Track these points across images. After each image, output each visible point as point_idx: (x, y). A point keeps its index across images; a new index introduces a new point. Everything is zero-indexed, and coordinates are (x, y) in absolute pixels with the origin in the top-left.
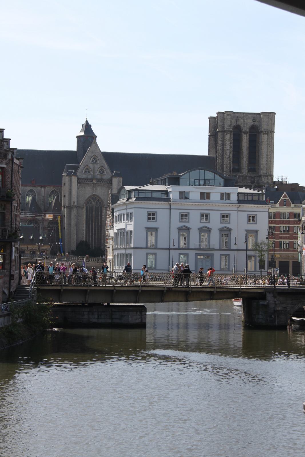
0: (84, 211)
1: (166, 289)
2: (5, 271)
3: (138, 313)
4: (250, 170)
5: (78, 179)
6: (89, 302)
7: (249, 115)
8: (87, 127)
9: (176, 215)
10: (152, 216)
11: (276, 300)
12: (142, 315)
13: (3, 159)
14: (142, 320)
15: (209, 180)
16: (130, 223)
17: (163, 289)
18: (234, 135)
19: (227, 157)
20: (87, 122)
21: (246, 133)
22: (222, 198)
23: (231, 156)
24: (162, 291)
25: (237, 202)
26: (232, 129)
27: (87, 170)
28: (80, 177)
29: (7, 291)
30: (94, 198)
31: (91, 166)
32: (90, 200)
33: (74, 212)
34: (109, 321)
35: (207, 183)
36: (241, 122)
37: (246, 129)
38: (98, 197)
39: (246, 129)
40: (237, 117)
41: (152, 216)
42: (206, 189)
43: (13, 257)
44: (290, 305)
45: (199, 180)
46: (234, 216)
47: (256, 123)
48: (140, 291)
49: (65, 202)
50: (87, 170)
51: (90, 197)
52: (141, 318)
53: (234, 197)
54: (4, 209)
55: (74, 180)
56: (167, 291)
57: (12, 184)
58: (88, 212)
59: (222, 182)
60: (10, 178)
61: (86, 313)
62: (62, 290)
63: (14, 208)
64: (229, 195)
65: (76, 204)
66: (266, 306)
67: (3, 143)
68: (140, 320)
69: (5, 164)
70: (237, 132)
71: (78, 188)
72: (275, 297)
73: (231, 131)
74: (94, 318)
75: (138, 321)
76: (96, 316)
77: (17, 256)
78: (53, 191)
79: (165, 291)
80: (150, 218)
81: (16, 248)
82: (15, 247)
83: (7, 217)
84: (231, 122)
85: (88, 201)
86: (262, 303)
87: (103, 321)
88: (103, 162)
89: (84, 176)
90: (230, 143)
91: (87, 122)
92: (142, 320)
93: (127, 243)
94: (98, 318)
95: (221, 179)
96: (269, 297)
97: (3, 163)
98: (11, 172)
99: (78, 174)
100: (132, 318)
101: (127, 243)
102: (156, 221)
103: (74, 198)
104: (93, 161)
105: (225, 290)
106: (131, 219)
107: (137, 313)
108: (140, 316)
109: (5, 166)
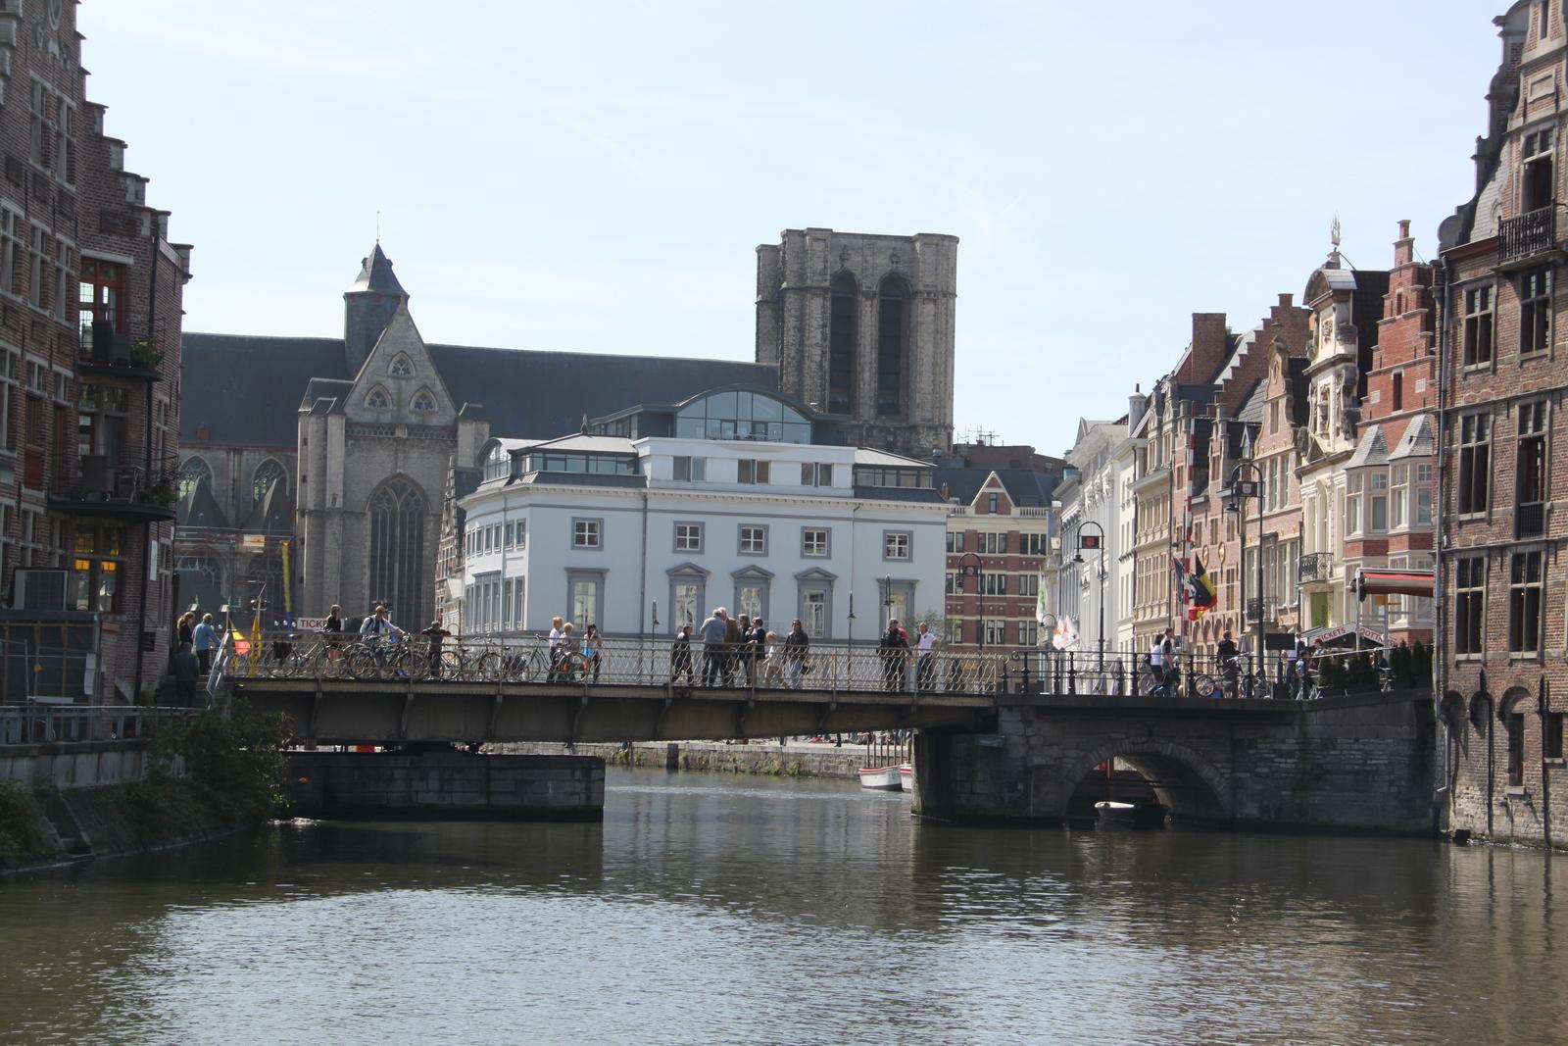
0: (367, 525)
1: (671, 693)
2: (125, 618)
3: (578, 774)
4: (882, 410)
5: (350, 426)
6: (412, 736)
7: (881, 243)
8: (380, 268)
9: (662, 530)
10: (586, 533)
11: (1029, 732)
12: (589, 782)
13: (121, 235)
14: (589, 798)
15: (766, 424)
16: (516, 554)
17: (661, 695)
18: (834, 301)
19: (814, 366)
20: (378, 250)
21: (870, 296)
22: (805, 479)
23: (826, 364)
24: (660, 702)
25: (851, 493)
26: (827, 284)
27: (379, 398)
28: (355, 419)
30: (399, 484)
31: (390, 384)
32: (385, 492)
33: (333, 528)
34: (481, 800)
35: (758, 431)
36: (854, 264)
37: (869, 283)
38: (412, 481)
39: (869, 283)
40: (845, 247)
41: (586, 533)
42: (756, 451)
43: (153, 576)
44: (1072, 753)
45: (735, 422)
46: (841, 534)
47: (902, 268)
48: (585, 701)
49: (306, 496)
50: (379, 398)
51: (385, 482)
52: (588, 789)
53: (842, 478)
54: (123, 406)
55: (336, 425)
56: (674, 700)
57: (151, 320)
58: (380, 529)
59: (806, 430)
60: (147, 302)
61: (398, 774)
62: (319, 695)
63: (160, 408)
64: (827, 469)
65: (339, 503)
66: (999, 753)
67: (121, 180)
68: (583, 796)
69: (128, 252)
70: (843, 293)
71: (348, 454)
72: (1027, 723)
73: (825, 290)
74: (428, 791)
75: (577, 801)
76: (434, 785)
77: (166, 576)
78: (265, 465)
79: (668, 702)
80: (580, 540)
81: (163, 545)
82: (158, 541)
83: (133, 436)
84: (825, 261)
85: (380, 495)
86: (986, 741)
87: (456, 799)
89: (368, 417)
90: (824, 326)
91: (378, 250)
92: (589, 798)
93: (506, 619)
94: (441, 791)
95: (804, 421)
96: (1009, 722)
97: (122, 251)
98: (148, 282)
99: (348, 409)
100: (555, 792)
101: (506, 619)
102: (601, 548)
104: (396, 370)
105: (864, 700)
106: (520, 540)
107: (573, 774)
108: (584, 785)
109: (130, 261)
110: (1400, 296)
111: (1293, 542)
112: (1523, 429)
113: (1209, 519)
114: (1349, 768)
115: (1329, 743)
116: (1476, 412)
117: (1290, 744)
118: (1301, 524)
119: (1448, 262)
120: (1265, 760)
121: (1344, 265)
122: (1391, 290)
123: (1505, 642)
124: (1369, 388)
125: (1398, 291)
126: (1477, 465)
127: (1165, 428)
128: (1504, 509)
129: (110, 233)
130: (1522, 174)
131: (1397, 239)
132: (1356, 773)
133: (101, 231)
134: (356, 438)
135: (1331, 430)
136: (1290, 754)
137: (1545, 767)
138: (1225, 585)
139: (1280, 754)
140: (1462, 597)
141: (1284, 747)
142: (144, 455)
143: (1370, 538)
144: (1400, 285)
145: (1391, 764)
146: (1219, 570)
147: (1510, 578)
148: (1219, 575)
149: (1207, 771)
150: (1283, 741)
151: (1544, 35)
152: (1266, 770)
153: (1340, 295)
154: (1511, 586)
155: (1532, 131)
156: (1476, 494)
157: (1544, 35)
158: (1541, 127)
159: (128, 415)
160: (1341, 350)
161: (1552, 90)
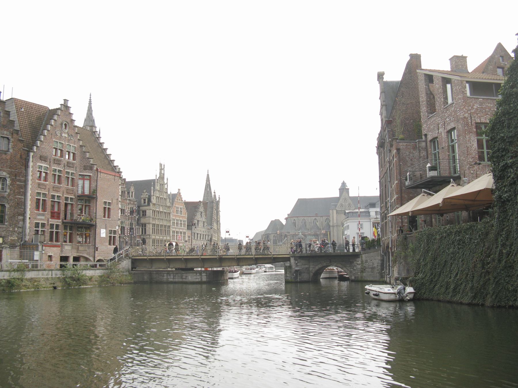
8: (344, 184)
13: (89, 170)
16: (348, 231)
27: (342, 205)
29: (92, 258)
31: (344, 204)
33: (335, 228)
34: (181, 280)
49: (331, 224)
52: (201, 277)
55: (335, 212)
61: (165, 275)
65: (336, 224)
67: (89, 159)
71: (337, 216)
74: (171, 278)
76: (172, 277)
78: (326, 219)
87: (177, 280)
88: (350, 201)
89: (340, 209)
94: (173, 278)
102: (363, 229)
103: (335, 221)
104: (344, 201)
107: (197, 274)
108: (200, 277)
109: (91, 174)
114: (370, 267)
115: (366, 261)
117: (359, 262)
129: (86, 170)
132: (371, 268)
133: (84, 169)
134: (338, 213)
141: (359, 263)
142: (95, 212)
150: (358, 262)
159: (91, 204)
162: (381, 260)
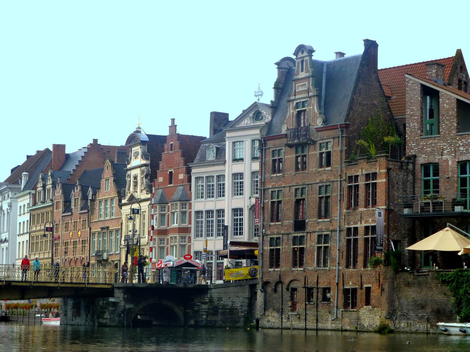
110: (172, 145)
111: (117, 231)
112: (296, 196)
113: (73, 221)
116: (276, 190)
118: (122, 224)
119: (264, 141)
120: (197, 305)
121: (142, 132)
122: (168, 142)
123: (290, 264)
124: (158, 175)
125: (171, 143)
126: (276, 206)
127: (47, 187)
128: (289, 222)
130: (295, 114)
131: (170, 125)
135: (139, 190)
136: (206, 303)
137: (306, 305)
138: (81, 246)
139: (203, 303)
140: (272, 250)
143: (159, 228)
144: (172, 141)
145: (242, 306)
146: (78, 240)
147: (291, 244)
148: (86, 241)
149: (177, 310)
151: (302, 71)
152: (197, 309)
153: (143, 143)
154: (292, 247)
155: (299, 101)
156: (275, 217)
157: (302, 71)
158: (302, 100)
160: (144, 162)
161: (306, 89)
162: (248, 298)
